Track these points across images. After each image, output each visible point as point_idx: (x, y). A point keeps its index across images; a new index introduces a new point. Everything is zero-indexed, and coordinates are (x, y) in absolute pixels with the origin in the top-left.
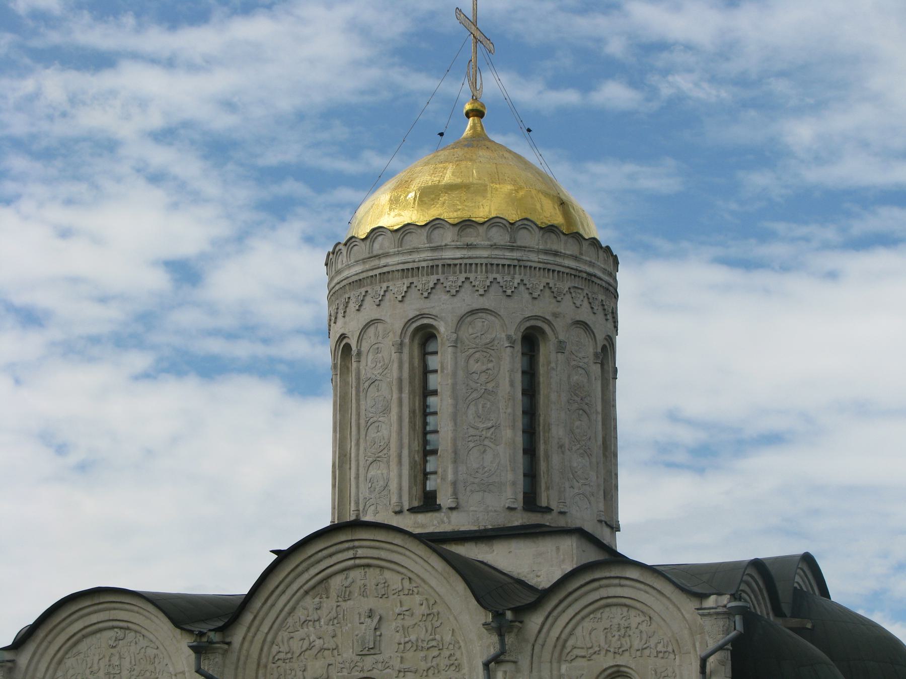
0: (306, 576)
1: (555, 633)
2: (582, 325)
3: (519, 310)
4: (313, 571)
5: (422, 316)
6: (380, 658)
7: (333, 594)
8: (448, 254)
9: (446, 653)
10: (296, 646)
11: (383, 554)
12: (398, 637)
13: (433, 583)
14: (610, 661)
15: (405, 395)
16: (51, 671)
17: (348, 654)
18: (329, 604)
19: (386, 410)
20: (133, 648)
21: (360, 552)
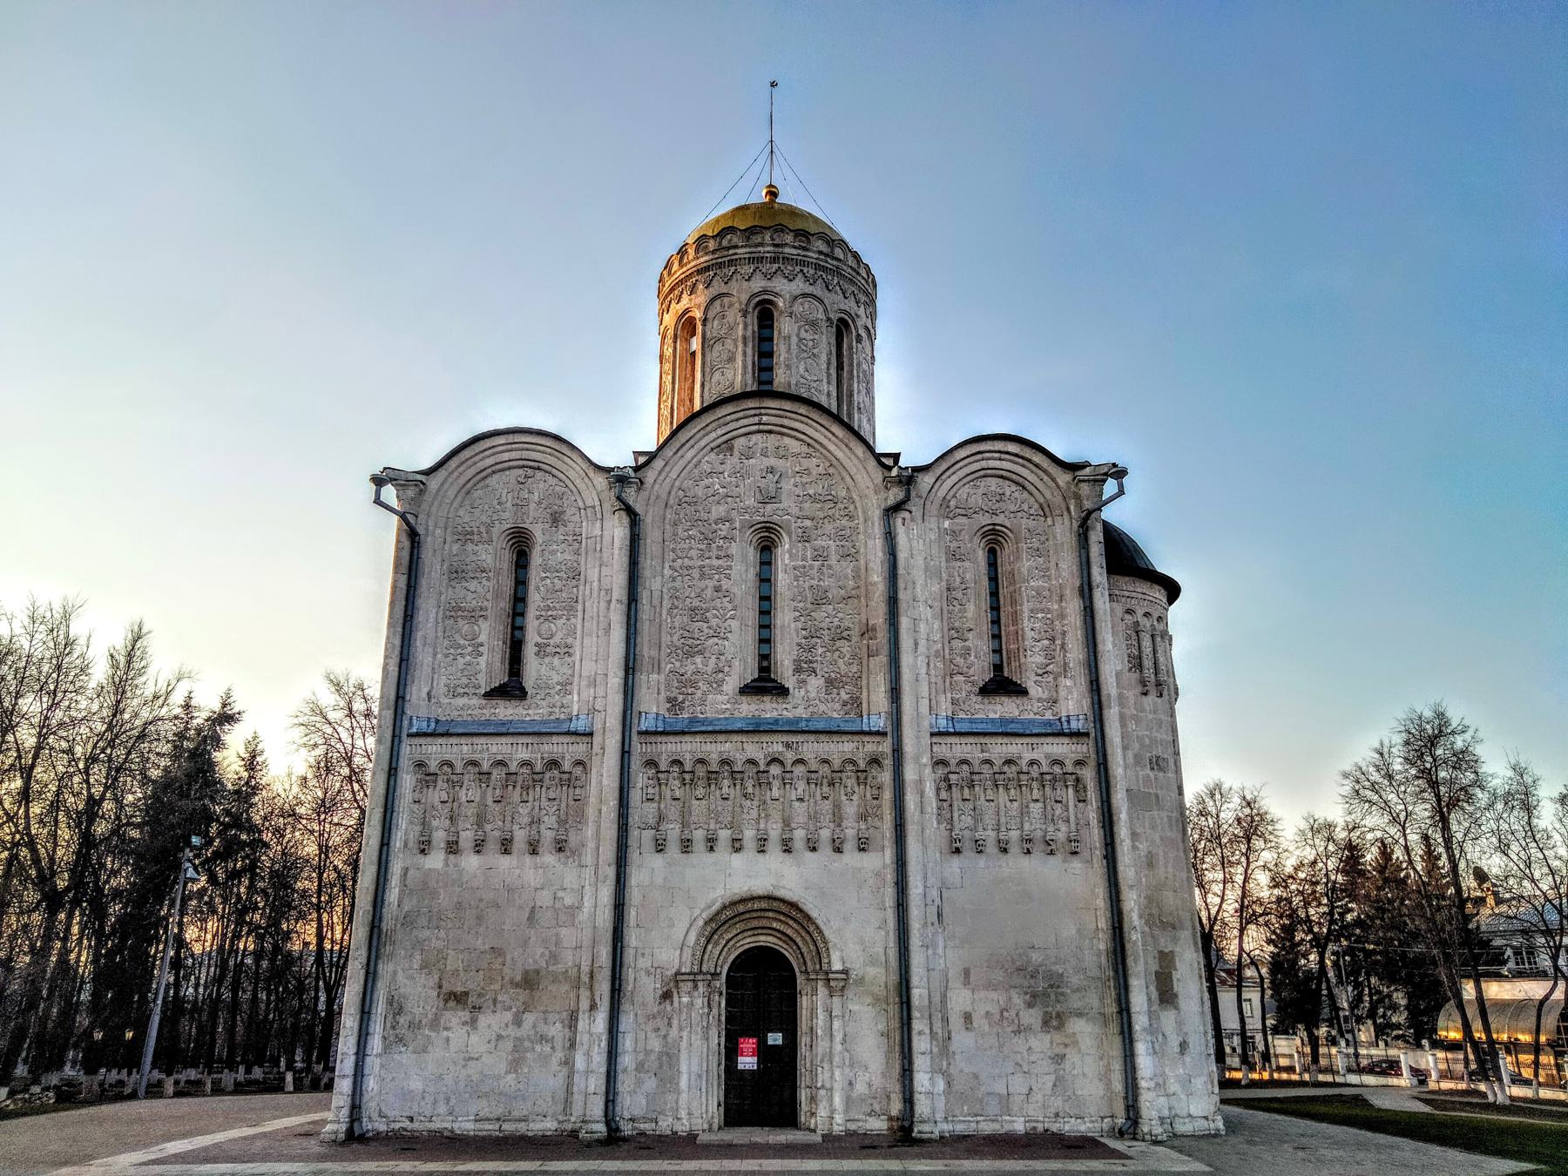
0: (713, 435)
1: (941, 493)
2: (867, 328)
3: (838, 302)
4: (720, 432)
5: (765, 291)
6: (781, 506)
7: (736, 452)
8: (787, 250)
9: (840, 505)
10: (700, 492)
11: (786, 422)
12: (798, 491)
13: (832, 448)
14: (986, 520)
15: (749, 351)
16: (459, 499)
17: (751, 502)
18: (733, 461)
19: (731, 359)
20: (542, 485)
21: (765, 419)
